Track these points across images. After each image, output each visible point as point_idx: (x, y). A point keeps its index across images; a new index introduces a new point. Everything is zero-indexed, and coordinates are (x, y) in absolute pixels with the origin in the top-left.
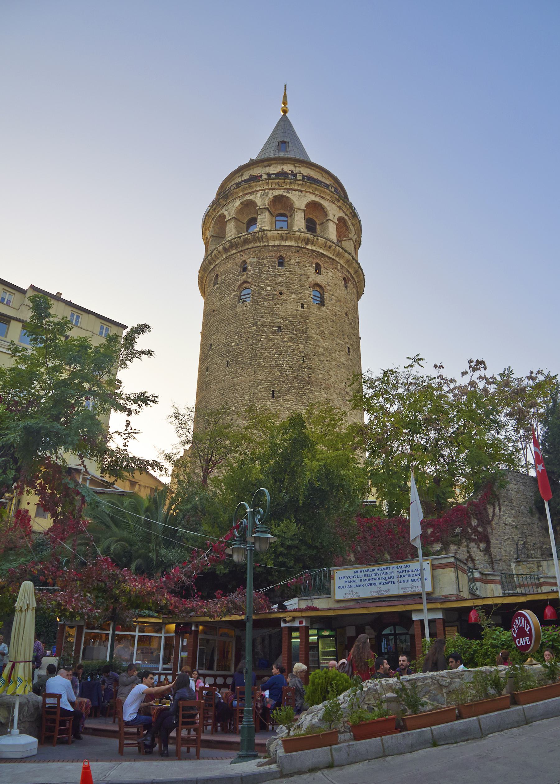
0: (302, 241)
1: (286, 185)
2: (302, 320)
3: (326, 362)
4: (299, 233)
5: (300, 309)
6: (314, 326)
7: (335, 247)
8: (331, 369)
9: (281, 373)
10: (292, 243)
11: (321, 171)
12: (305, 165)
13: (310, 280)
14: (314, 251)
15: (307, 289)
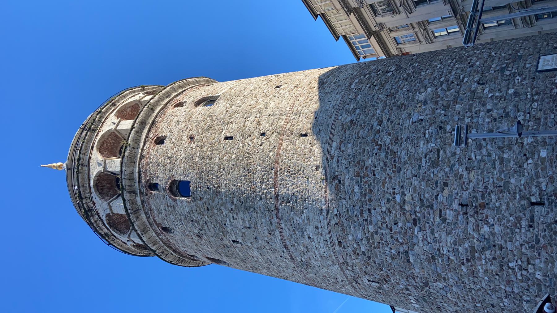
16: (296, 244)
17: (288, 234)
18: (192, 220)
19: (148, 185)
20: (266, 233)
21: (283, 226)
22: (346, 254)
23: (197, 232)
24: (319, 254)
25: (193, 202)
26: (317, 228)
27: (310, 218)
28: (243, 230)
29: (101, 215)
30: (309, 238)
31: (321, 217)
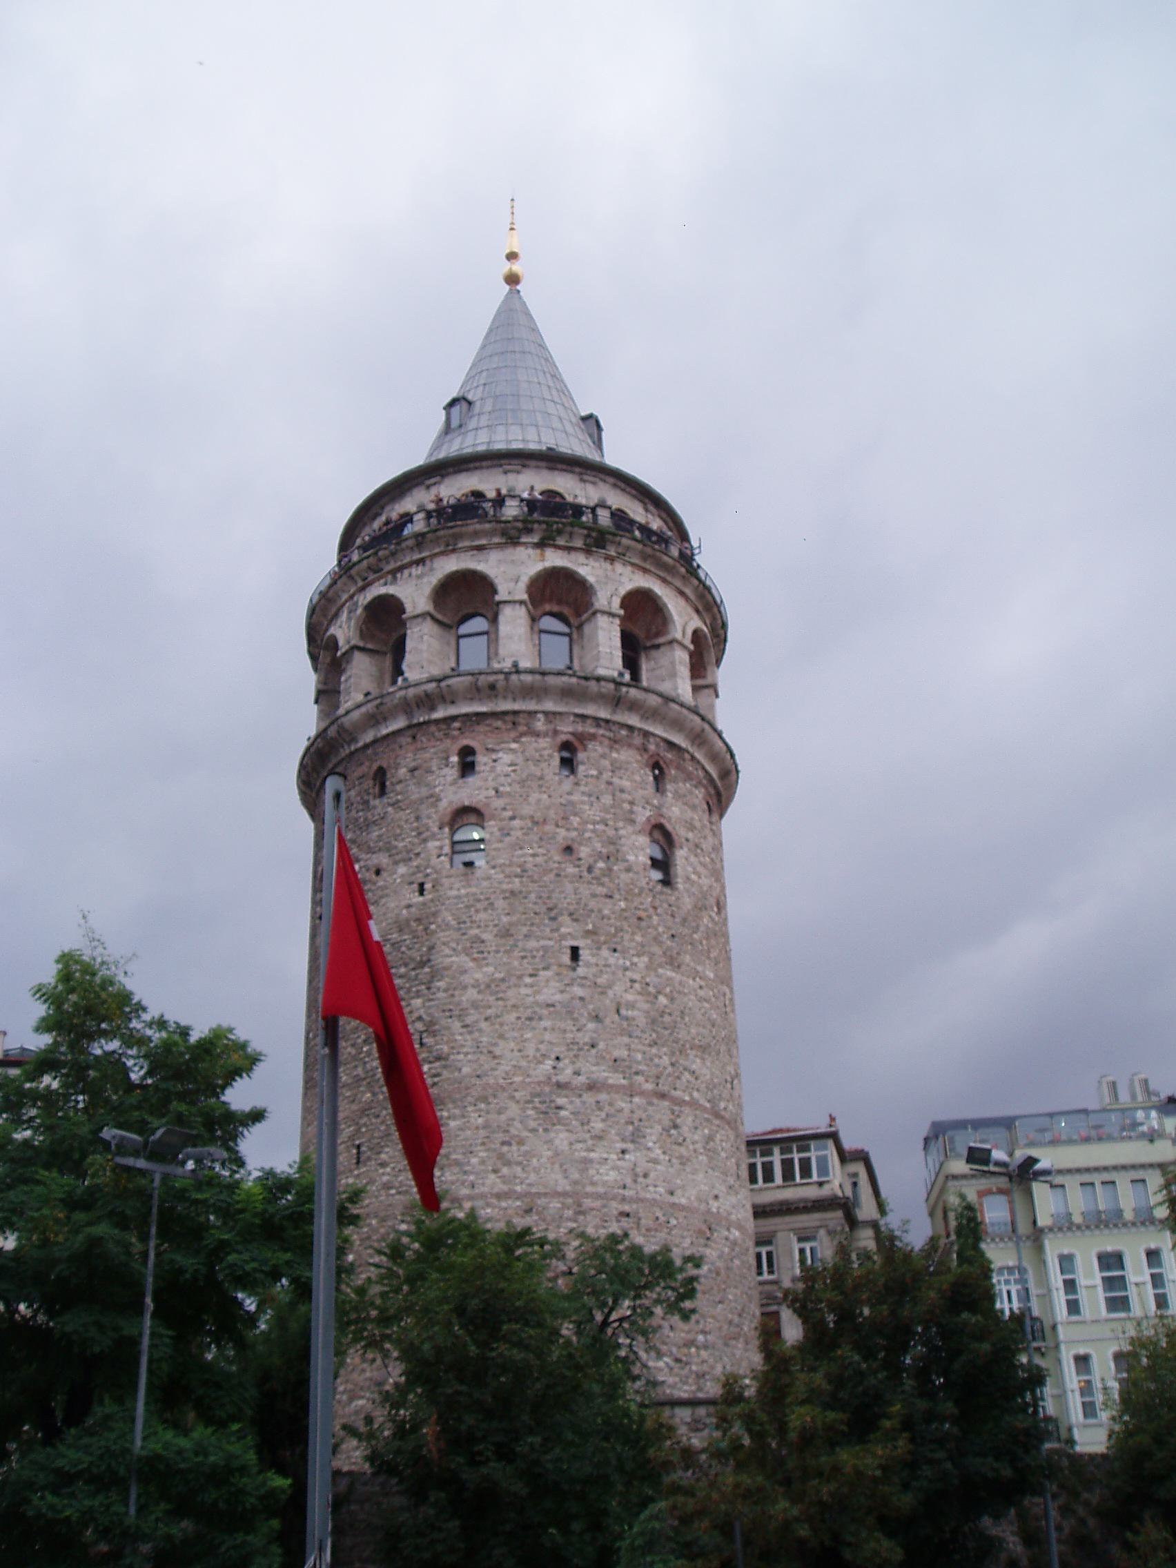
0: (418, 706)
1: (388, 563)
2: (421, 927)
3: (483, 1025)
4: (402, 693)
5: (418, 899)
6: (456, 935)
7: (507, 679)
8: (501, 1037)
9: (374, 1094)
10: (399, 723)
11: (495, 462)
12: (451, 470)
13: (443, 804)
14: (454, 718)
15: (434, 837)
16: (603, 1115)
17: (624, 1105)
18: (612, 859)
19: (661, 763)
20: (616, 1054)
21: (636, 1100)
22: (606, 1221)
23: (582, 855)
24: (591, 1161)
25: (648, 883)
26: (645, 1176)
27: (659, 1167)
28: (610, 993)
29: (581, 557)
30: (623, 1152)
31: (661, 1190)
